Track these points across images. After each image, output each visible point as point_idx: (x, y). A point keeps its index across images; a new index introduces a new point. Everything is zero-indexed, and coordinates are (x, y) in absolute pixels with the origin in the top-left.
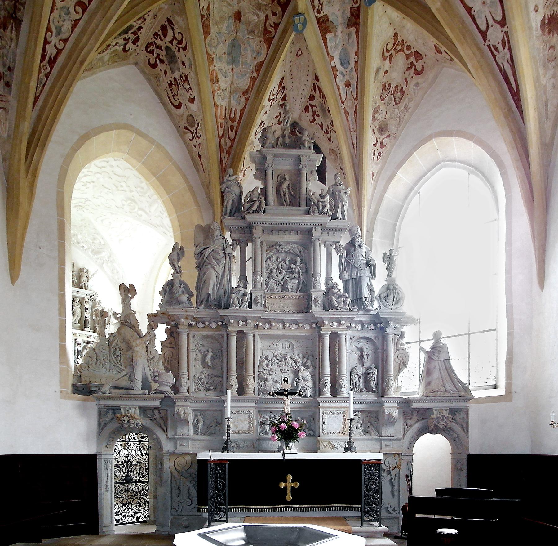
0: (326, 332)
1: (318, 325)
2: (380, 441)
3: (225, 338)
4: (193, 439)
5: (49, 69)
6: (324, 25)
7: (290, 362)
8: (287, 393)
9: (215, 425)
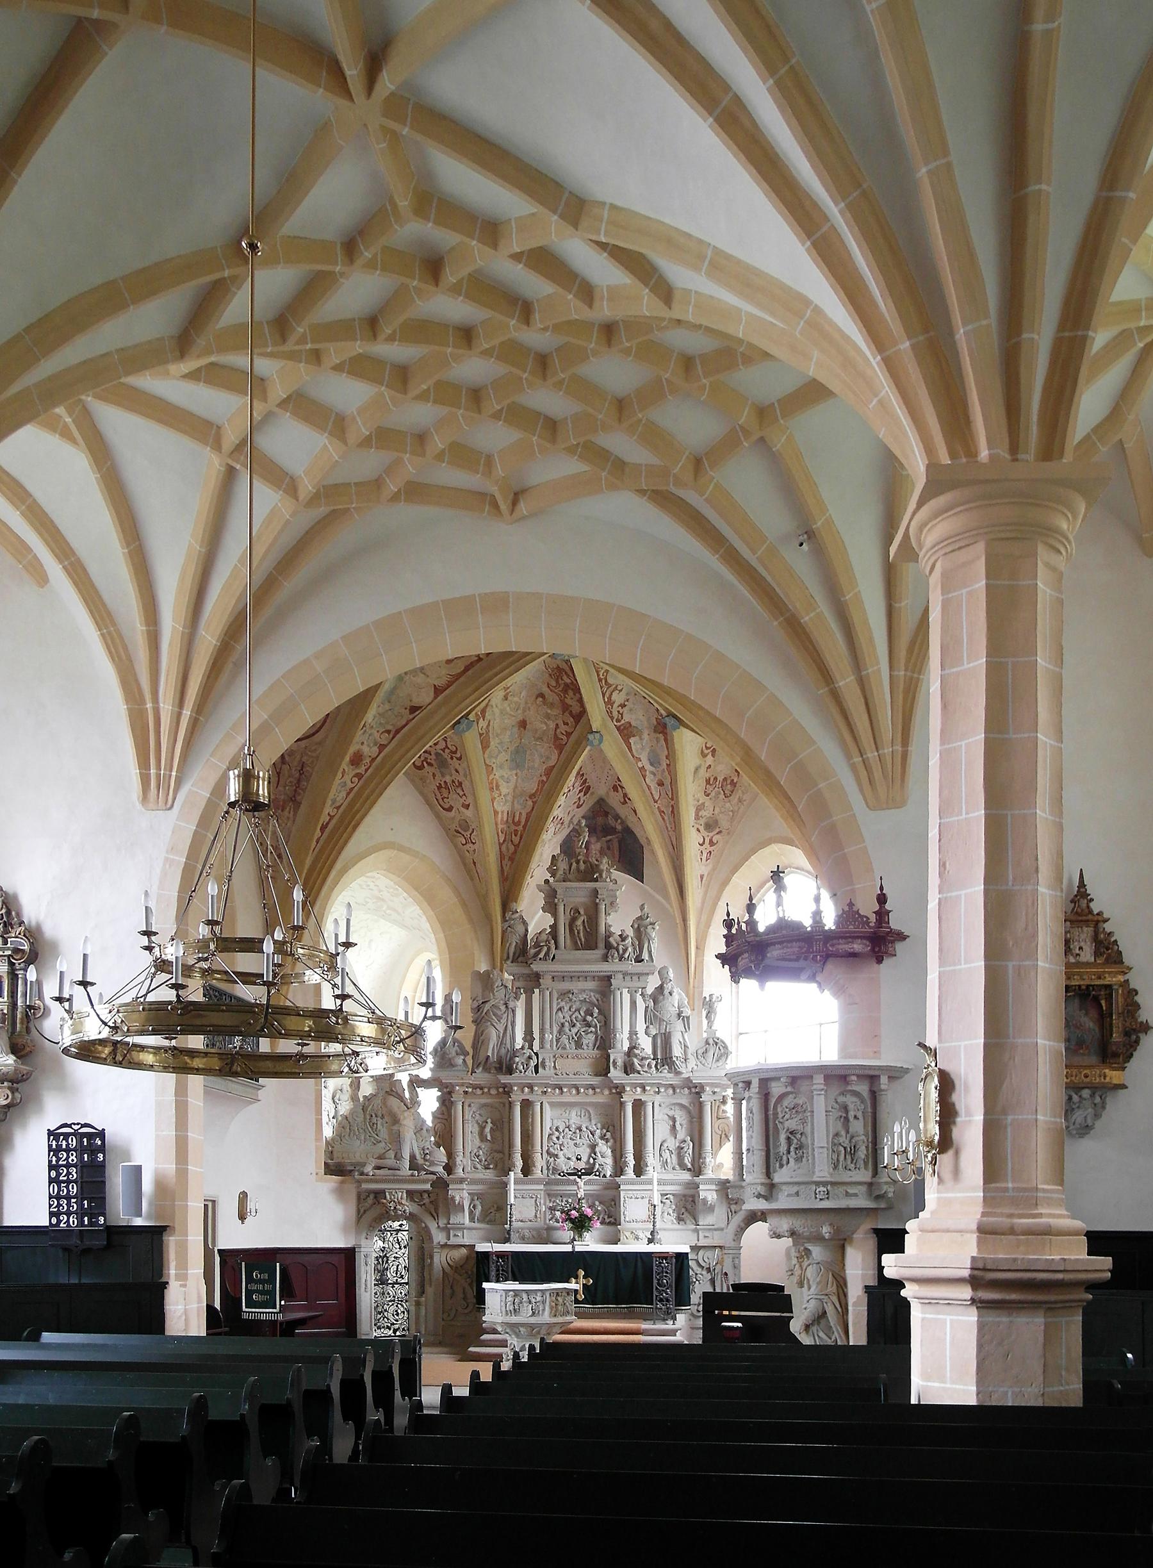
1: (619, 1090)
2: (697, 1231)
4: (469, 1229)
6: (626, 732)
7: (586, 1133)
9: (494, 1210)
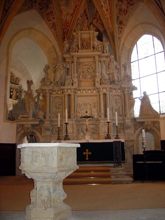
0: (101, 93)
3: (64, 97)
5: (6, 13)
8: (87, 117)
